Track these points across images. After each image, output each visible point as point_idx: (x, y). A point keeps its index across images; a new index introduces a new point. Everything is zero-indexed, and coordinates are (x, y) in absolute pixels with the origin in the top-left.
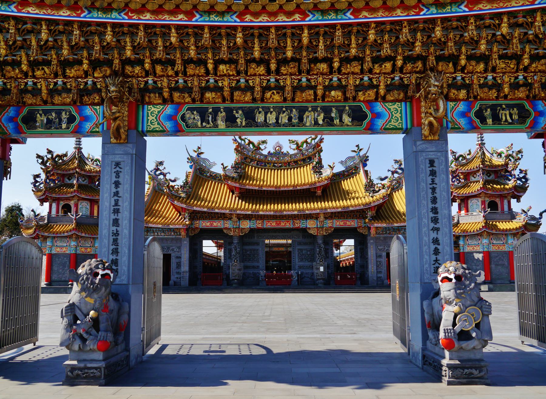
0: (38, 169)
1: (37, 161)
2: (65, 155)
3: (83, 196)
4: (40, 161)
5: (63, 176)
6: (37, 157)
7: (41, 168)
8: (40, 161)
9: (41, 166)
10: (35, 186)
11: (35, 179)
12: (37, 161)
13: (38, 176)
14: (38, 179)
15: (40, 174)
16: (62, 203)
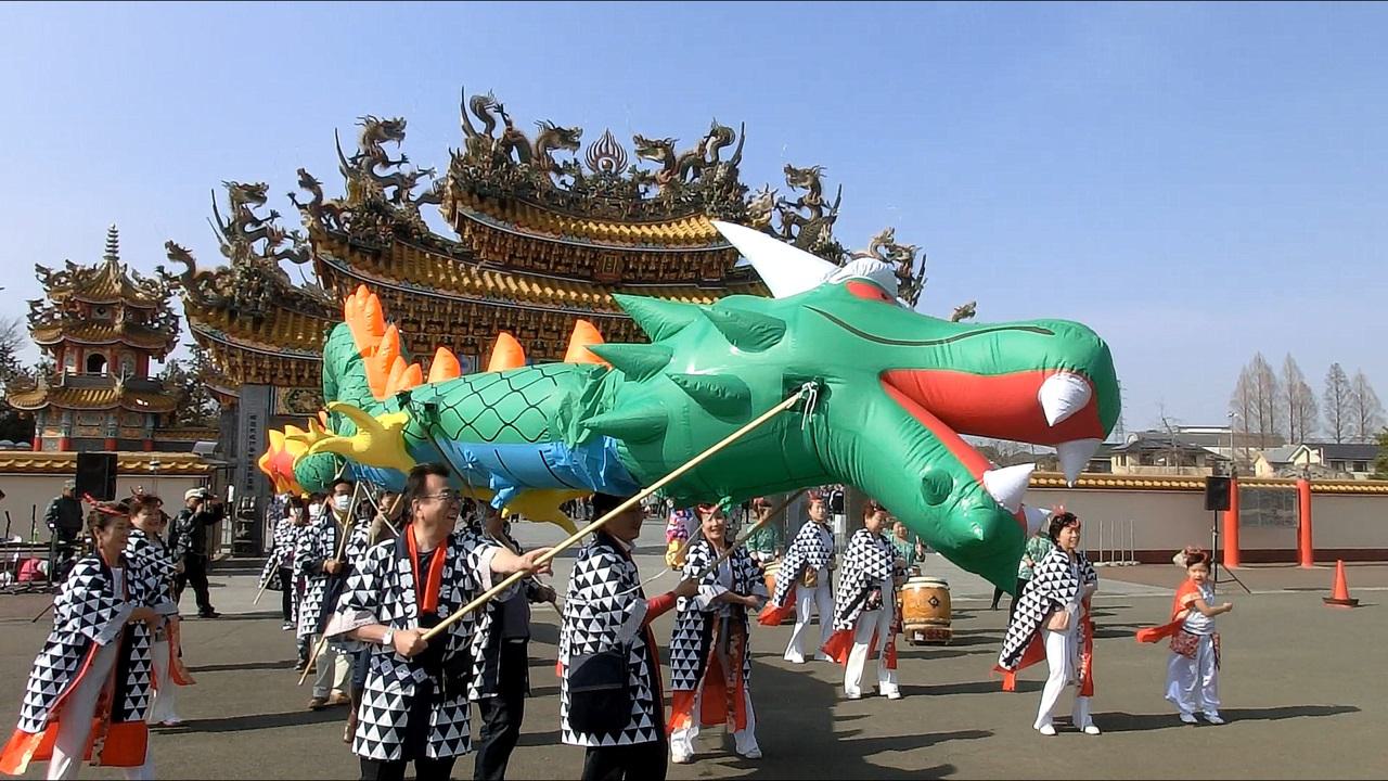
0: (38, 291)
1: (37, 276)
2: (94, 270)
3: (131, 343)
4: (43, 277)
5: (91, 306)
6: (37, 270)
7: (45, 290)
8: (43, 277)
9: (44, 286)
10: (32, 321)
11: (32, 308)
12: (37, 276)
13: (38, 303)
14: (38, 309)
15: (42, 300)
16: (88, 353)
